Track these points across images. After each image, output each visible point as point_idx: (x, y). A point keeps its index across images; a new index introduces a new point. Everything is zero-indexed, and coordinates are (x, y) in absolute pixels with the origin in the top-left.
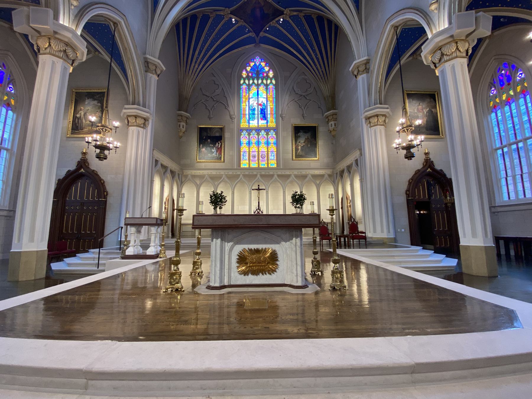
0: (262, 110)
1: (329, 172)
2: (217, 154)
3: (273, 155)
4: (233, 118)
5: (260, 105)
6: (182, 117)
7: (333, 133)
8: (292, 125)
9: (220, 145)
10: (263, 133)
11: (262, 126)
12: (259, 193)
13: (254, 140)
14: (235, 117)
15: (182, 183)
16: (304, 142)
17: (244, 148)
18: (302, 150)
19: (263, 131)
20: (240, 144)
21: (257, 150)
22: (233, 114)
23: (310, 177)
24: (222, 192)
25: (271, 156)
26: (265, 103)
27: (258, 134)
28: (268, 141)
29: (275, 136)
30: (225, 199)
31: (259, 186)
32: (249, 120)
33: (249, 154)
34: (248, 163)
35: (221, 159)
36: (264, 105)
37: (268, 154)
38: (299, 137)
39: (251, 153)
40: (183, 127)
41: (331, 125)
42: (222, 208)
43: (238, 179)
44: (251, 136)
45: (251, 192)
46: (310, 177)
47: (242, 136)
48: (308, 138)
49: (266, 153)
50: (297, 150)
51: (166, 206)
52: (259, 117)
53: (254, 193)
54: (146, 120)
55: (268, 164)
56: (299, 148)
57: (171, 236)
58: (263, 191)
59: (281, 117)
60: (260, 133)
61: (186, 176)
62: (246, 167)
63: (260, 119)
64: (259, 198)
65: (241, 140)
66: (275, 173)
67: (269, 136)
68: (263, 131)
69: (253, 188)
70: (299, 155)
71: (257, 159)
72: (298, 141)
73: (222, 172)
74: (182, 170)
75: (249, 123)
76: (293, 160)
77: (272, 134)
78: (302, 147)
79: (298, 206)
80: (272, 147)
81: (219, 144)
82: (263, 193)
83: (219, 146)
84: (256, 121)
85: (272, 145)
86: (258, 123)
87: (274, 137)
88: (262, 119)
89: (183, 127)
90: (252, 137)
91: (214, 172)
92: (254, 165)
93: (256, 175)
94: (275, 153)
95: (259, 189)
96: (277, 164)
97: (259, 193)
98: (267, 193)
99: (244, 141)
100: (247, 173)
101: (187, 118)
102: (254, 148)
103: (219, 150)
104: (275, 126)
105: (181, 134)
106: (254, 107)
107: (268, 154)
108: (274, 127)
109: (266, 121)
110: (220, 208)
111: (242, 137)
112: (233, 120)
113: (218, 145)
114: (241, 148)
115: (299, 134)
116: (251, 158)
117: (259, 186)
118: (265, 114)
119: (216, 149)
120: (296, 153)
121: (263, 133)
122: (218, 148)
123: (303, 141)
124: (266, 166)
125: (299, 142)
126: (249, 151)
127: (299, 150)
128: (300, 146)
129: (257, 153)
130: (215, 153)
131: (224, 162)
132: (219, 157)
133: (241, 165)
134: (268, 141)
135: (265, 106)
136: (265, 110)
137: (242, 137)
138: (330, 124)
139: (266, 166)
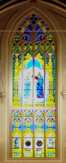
0: (38, 84)
5: (37, 78)
14: (4, 95)
22: (4, 91)
26: (43, 76)
34: (21, 152)
36: (42, 78)
59: (62, 95)
87: (53, 119)
88: (39, 97)
106: (28, 81)
109: (43, 99)
118: (42, 90)
133: (13, 154)
135: (42, 79)
136: (42, 84)
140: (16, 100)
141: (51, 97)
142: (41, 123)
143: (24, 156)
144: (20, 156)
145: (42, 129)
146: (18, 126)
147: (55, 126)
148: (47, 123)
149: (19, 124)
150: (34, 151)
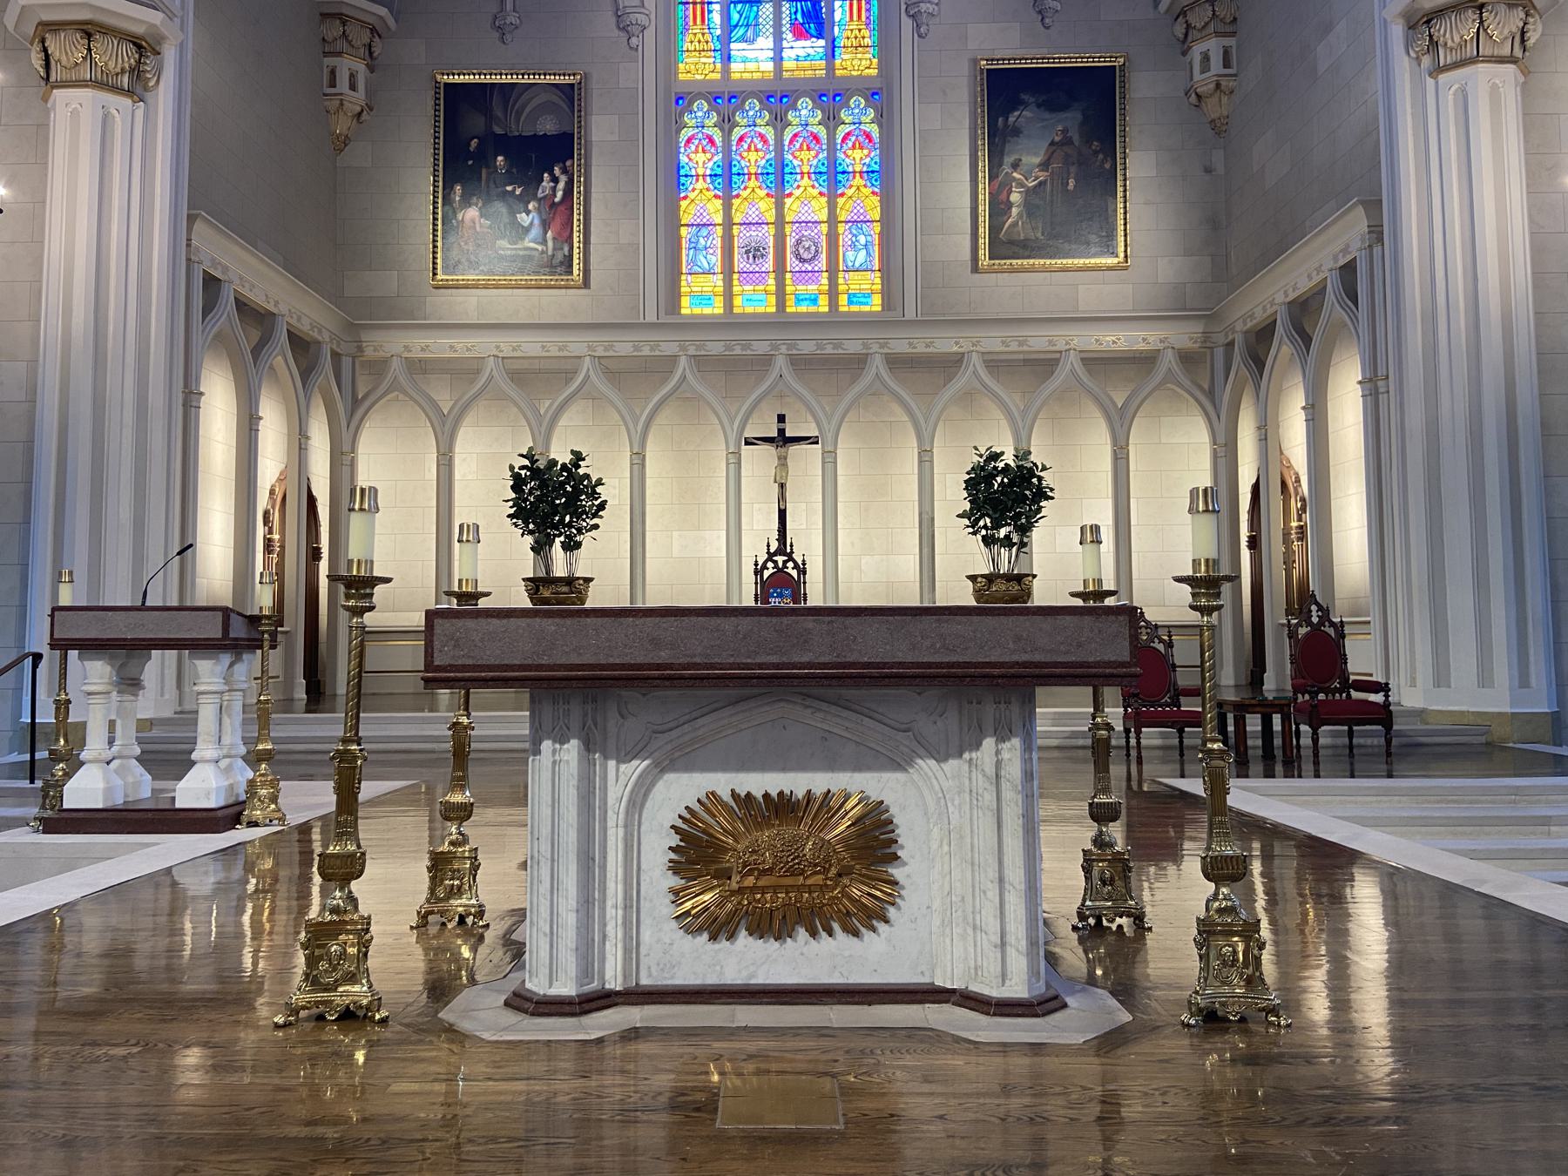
1: (1183, 335)
2: (544, 242)
3: (862, 239)
4: (635, 29)
6: (344, 23)
7: (1213, 108)
8: (975, 61)
9: (561, 185)
10: (805, 113)
11: (801, 74)
12: (783, 462)
13: (753, 156)
14: (642, 19)
15: (356, 403)
16: (1044, 166)
17: (700, 203)
18: (1029, 207)
19: (805, 104)
20: (673, 180)
21: (771, 216)
23: (1073, 371)
24: (578, 457)
25: (853, 246)
27: (779, 122)
28: (832, 162)
29: (874, 130)
30: (594, 495)
31: (781, 419)
32: (726, 39)
33: (728, 239)
35: (571, 266)
37: (833, 238)
38: (1016, 132)
39: (736, 230)
40: (353, 87)
41: (1206, 58)
42: (578, 545)
43: (665, 381)
44: (737, 133)
45: (738, 454)
46: (1073, 371)
47: (685, 134)
48: (1067, 141)
49: (824, 228)
50: (999, 208)
51: (270, 532)
52: (786, 21)
53: (757, 463)
54: (144, 46)
55: (833, 293)
56: (1015, 197)
57: (305, 696)
58: (804, 447)
60: (791, 116)
61: (379, 367)
62: (708, 311)
63: (786, 27)
64: (782, 486)
65: (683, 159)
66: (875, 348)
67: (841, 131)
68: (805, 104)
69: (750, 433)
70: (1011, 242)
71: (769, 264)
72: (1008, 160)
73: (577, 344)
74: (353, 329)
75: (727, 59)
76: (975, 268)
77: (858, 115)
78: (1029, 193)
79: (1003, 532)
80: (863, 200)
81: (555, 180)
82: (806, 460)
83: (560, 194)
84: (766, 42)
85: (858, 181)
86: (778, 59)
87: (868, 136)
88: (800, 33)
89: (353, 87)
90: (741, 139)
91: (531, 346)
92: (755, 300)
93: (766, 361)
94: (877, 228)
95: (782, 440)
96: (886, 293)
97: (783, 462)
98: (829, 459)
99: (698, 161)
100: (716, 349)
101: (373, 30)
102: (755, 202)
103: (559, 214)
104: (874, 72)
105: (342, 126)
107: (833, 238)
108: (869, 77)
109: (822, 42)
110: (571, 546)
111: (689, 141)
112: (634, 41)
113: (554, 189)
114: (684, 204)
115: (1011, 119)
116: (740, 263)
117: (781, 419)
119: (539, 210)
120: (994, 230)
121: (805, 113)
122: (553, 205)
123: (1037, 160)
124: (823, 306)
125: (1015, 166)
126: (728, 223)
127: (1015, 211)
128: (1021, 185)
129: (772, 230)
130: (536, 232)
131: (586, 284)
132: (559, 256)
133: (685, 301)
134: (832, 162)
137: (689, 141)
138: (1197, 50)
139: (823, 306)
140: (695, 51)
141: (860, 30)
142: (813, 153)
143: (736, 310)
144: (717, 308)
145: (817, 180)
146: (708, 172)
147: (876, 168)
148: (840, 155)
149: (709, 160)
150: (781, 285)
